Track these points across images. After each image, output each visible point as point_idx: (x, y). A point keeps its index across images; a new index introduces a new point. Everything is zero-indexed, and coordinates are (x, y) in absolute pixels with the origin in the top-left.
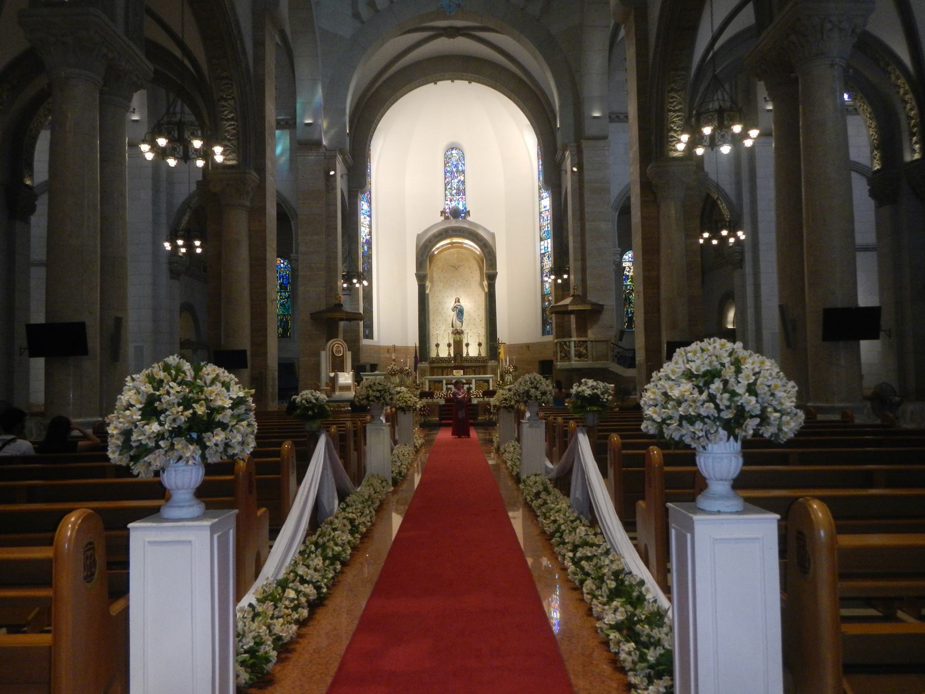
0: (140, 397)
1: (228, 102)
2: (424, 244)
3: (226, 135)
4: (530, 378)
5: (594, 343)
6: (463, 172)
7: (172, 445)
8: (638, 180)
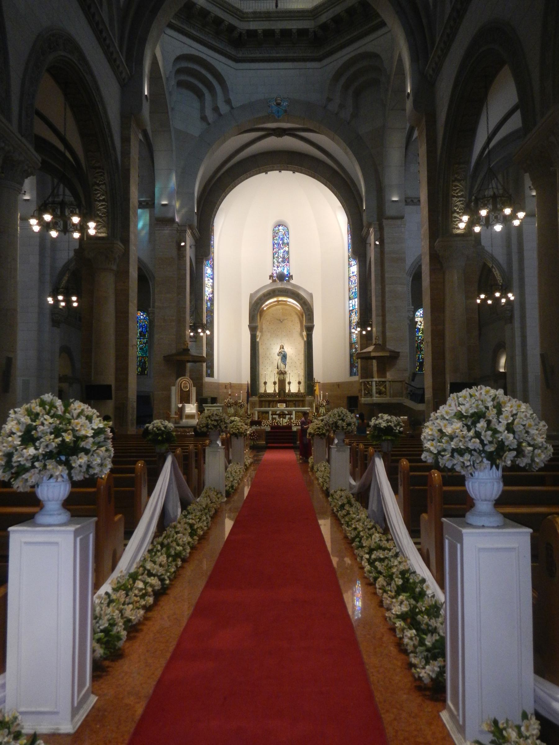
0: (20, 427)
1: (101, 187)
2: (255, 302)
3: (99, 213)
4: (338, 412)
5: (391, 382)
6: (288, 244)
7: (45, 466)
8: (428, 252)
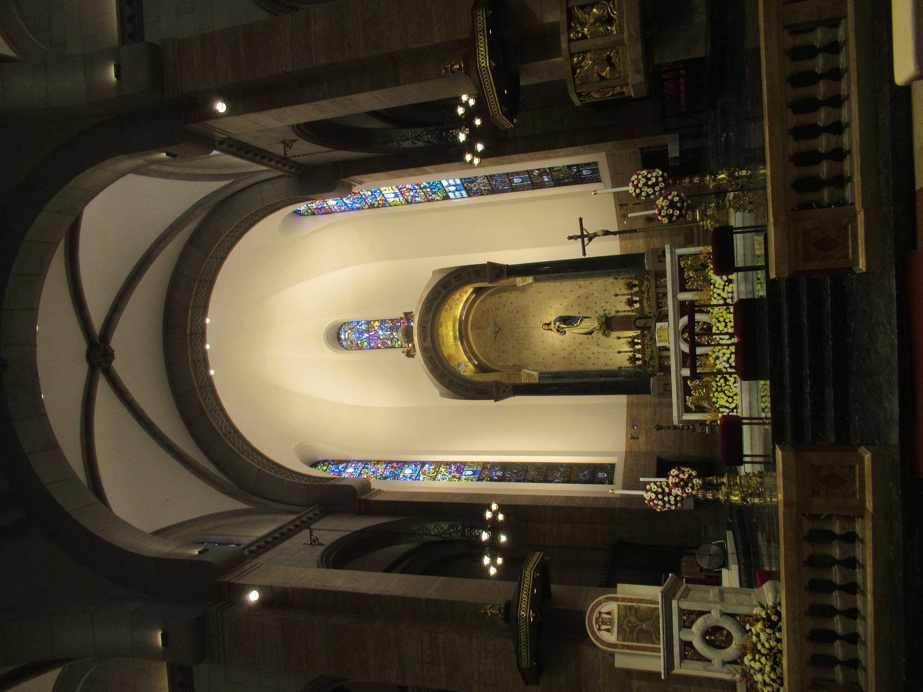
2: (448, 387)
6: (368, 323)
